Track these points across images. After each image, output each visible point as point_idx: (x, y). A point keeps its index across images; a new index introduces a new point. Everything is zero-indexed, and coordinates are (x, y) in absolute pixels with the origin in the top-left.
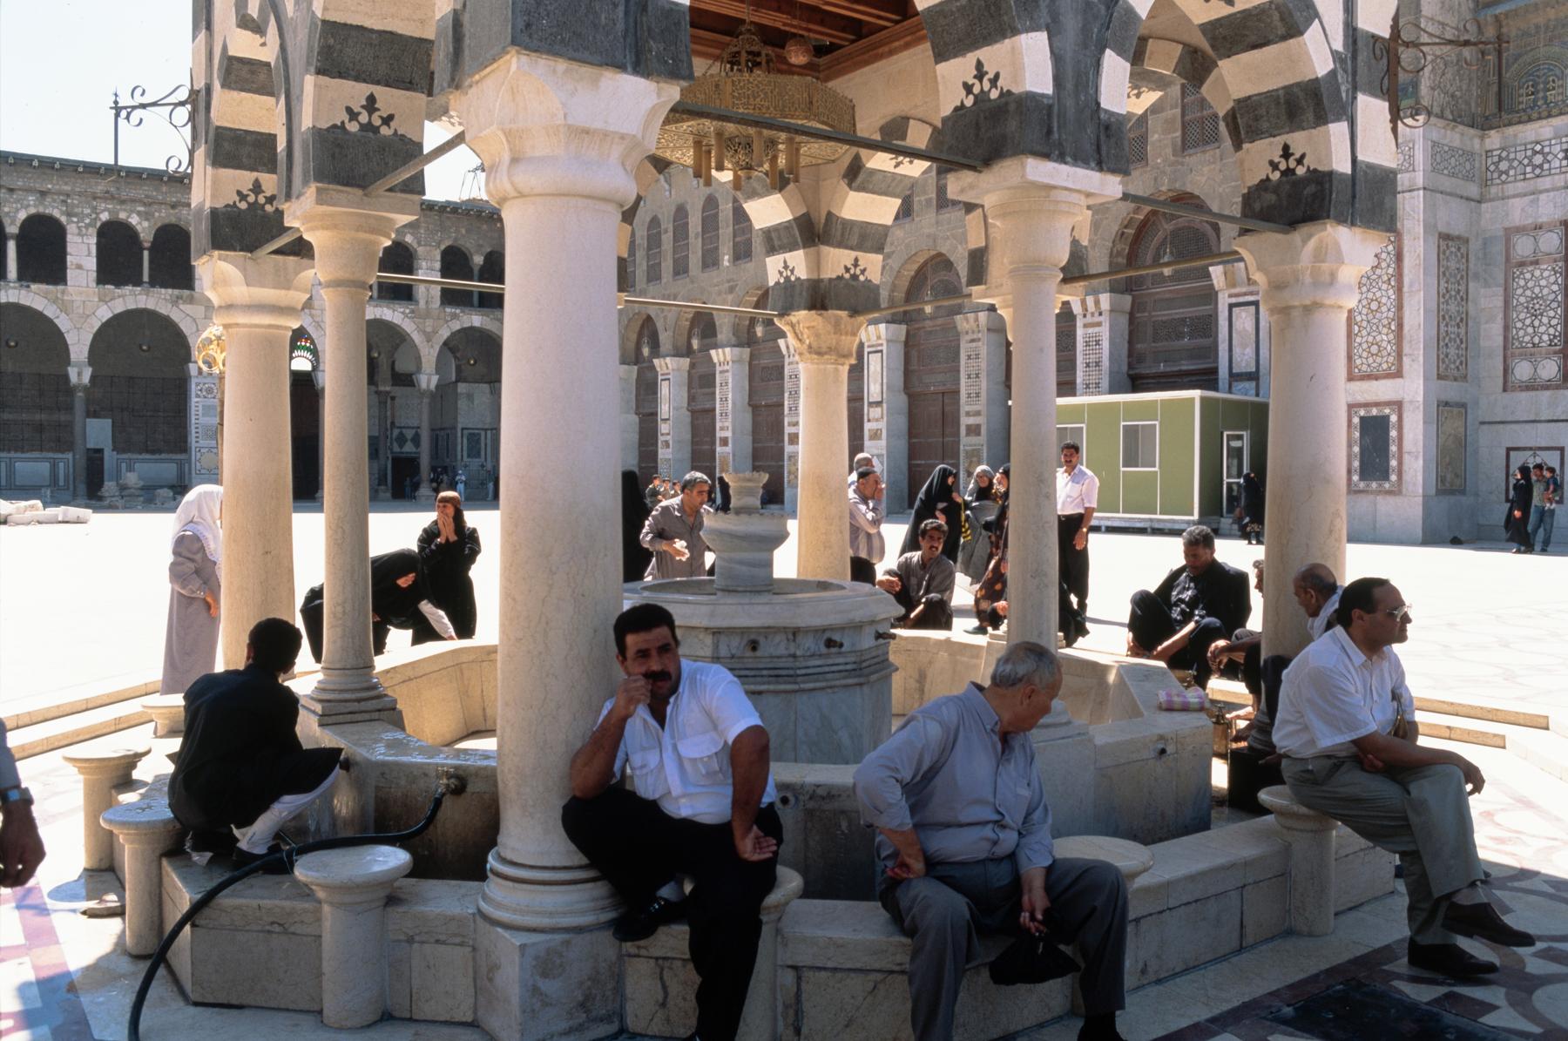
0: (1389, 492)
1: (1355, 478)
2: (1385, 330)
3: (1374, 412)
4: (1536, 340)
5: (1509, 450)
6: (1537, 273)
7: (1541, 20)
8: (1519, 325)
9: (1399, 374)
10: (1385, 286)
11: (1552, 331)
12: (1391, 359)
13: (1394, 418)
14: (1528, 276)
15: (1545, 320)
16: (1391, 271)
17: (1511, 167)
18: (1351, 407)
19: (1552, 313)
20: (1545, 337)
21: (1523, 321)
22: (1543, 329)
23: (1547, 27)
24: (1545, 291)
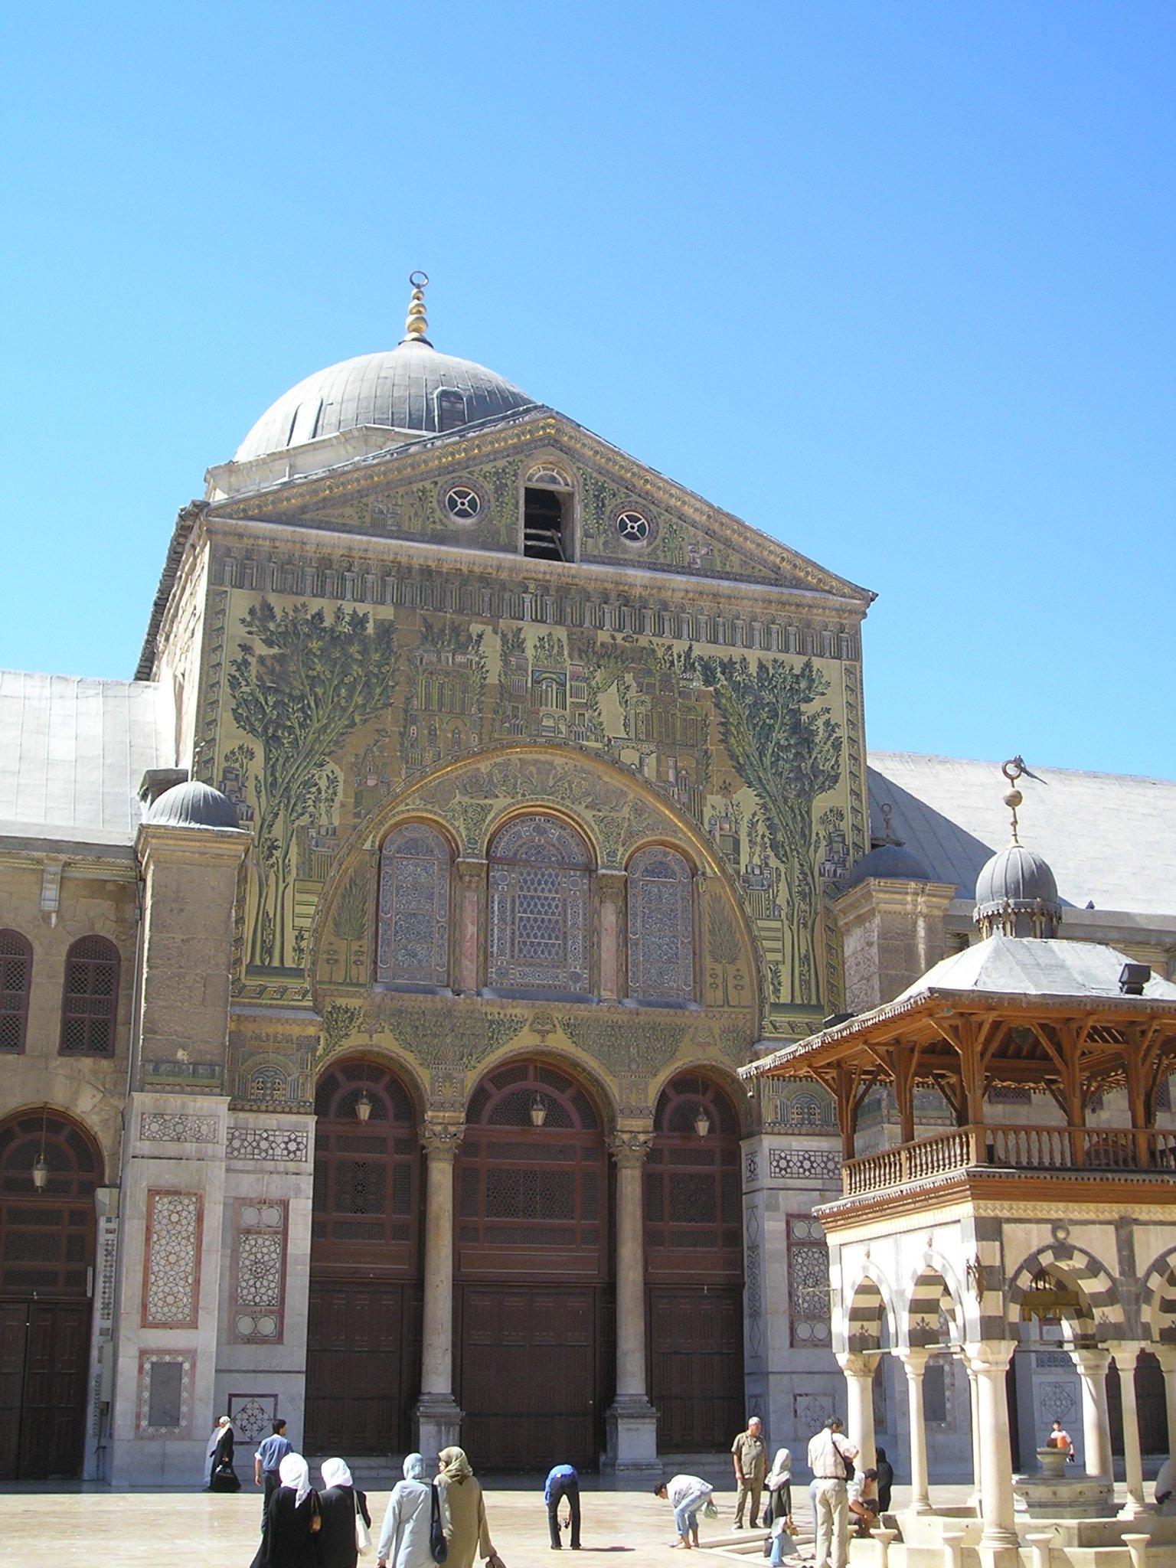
0: (182, 1438)
1: (144, 1423)
2: (182, 1283)
3: (167, 1358)
4: (257, 1299)
5: (231, 1396)
6: (260, 1241)
7: (271, 1030)
8: (244, 1284)
9: (194, 1325)
10: (184, 1242)
11: (270, 1292)
12: (187, 1311)
13: (186, 1366)
14: (253, 1242)
15: (265, 1283)
16: (191, 1229)
17: (242, 1145)
18: (143, 1353)
19: (271, 1278)
20: (265, 1298)
21: (247, 1281)
22: (263, 1290)
23: (275, 1037)
24: (266, 1258)
